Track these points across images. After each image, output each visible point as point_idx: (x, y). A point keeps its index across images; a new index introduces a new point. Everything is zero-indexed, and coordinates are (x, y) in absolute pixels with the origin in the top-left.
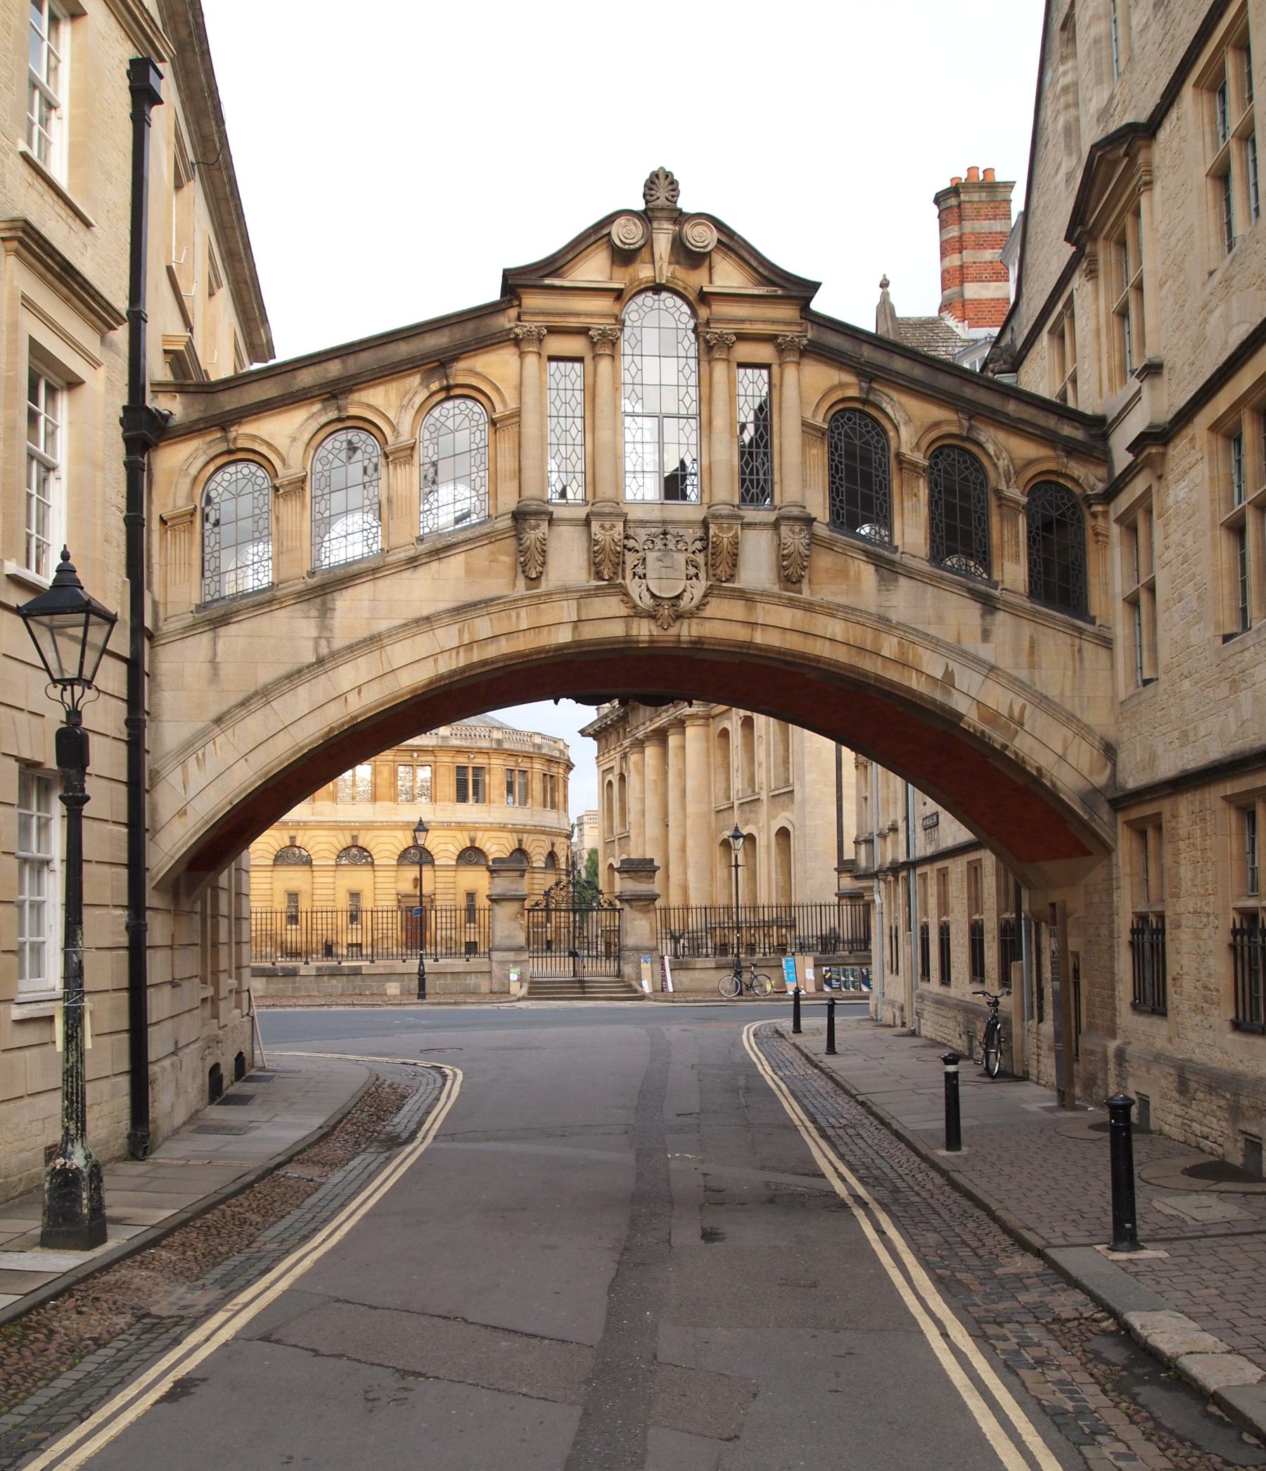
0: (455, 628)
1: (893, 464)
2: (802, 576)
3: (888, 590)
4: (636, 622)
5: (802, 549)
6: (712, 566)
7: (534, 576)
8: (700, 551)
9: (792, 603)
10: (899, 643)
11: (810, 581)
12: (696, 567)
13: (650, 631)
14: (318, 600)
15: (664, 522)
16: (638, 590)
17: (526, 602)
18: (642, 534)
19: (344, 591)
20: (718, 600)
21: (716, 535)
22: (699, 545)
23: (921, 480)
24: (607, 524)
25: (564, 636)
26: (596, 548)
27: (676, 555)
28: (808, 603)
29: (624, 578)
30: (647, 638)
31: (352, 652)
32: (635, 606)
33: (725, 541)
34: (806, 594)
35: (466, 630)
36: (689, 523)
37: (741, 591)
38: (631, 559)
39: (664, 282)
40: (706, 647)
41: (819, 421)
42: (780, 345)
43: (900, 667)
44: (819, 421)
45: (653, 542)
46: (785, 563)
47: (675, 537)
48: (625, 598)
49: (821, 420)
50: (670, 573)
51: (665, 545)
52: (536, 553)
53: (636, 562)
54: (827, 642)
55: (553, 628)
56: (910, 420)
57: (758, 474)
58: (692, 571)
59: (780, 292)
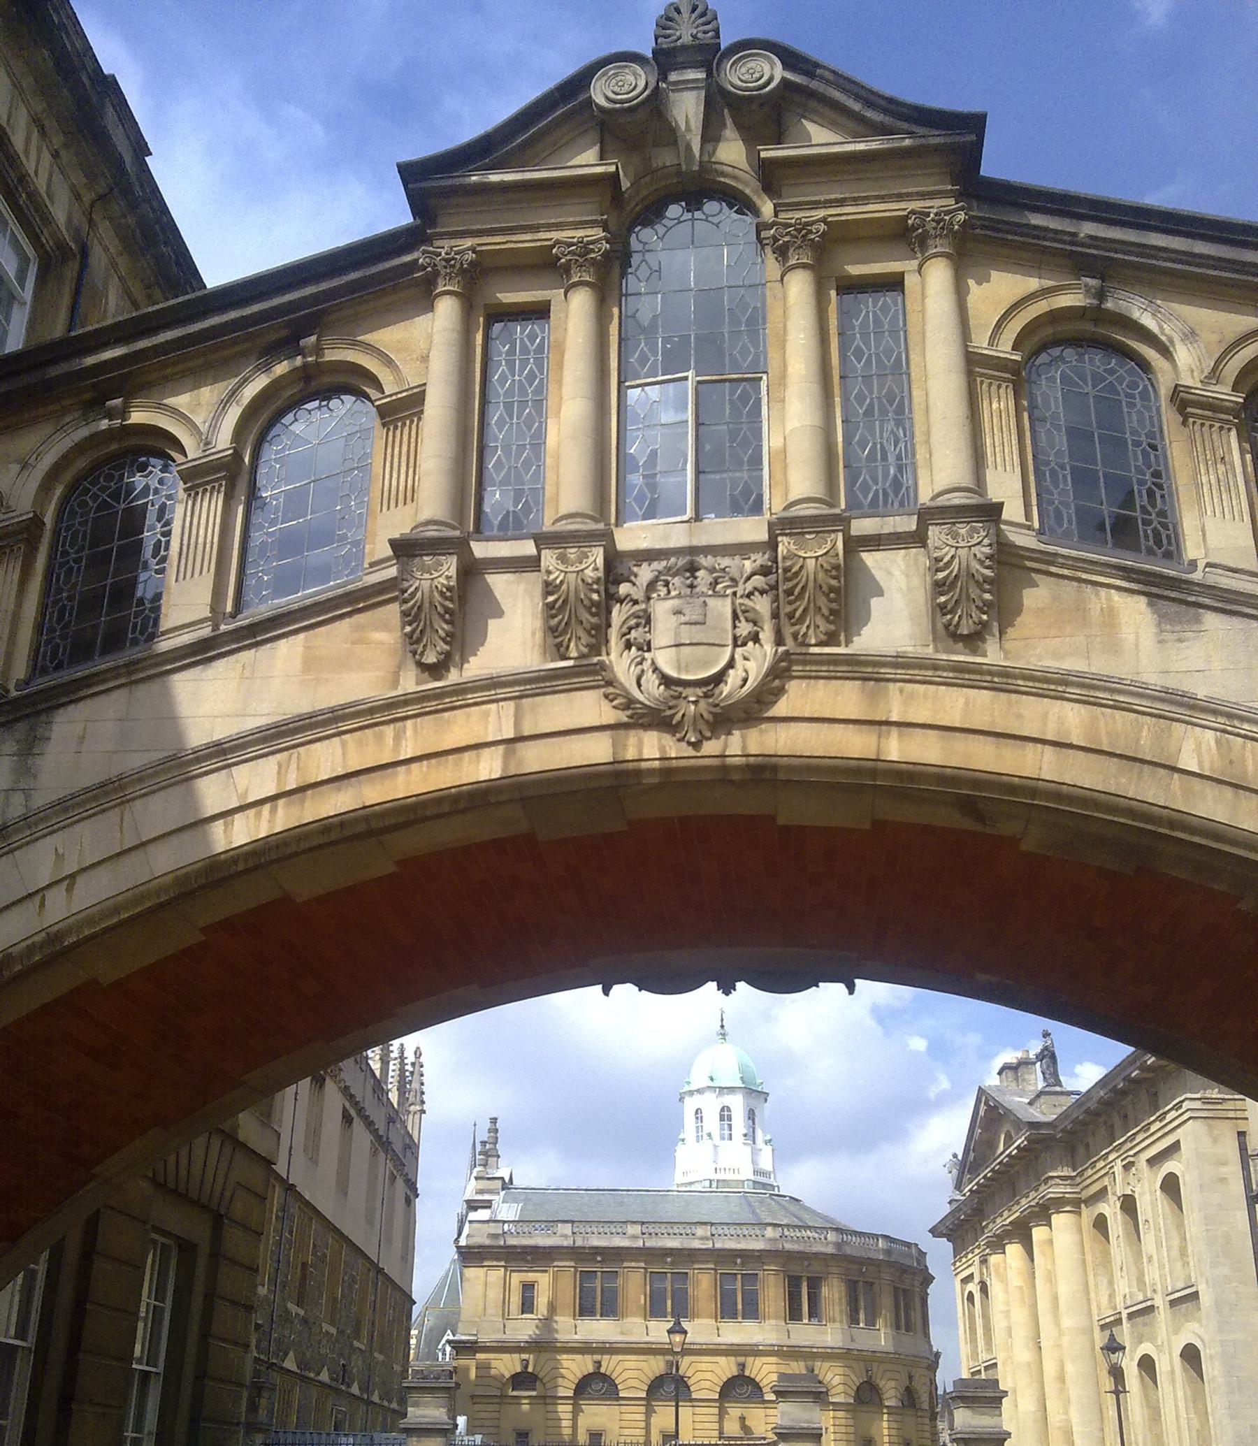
0: (272, 761)
1: (1169, 417)
2: (985, 625)
3: (1180, 640)
4: (632, 737)
5: (975, 566)
6: (791, 616)
7: (431, 658)
8: (762, 592)
9: (966, 676)
10: (1218, 742)
11: (1001, 633)
12: (755, 623)
13: (662, 748)
14: (21, 727)
15: (693, 550)
16: (635, 671)
17: (412, 710)
18: (645, 573)
19: (71, 707)
20: (804, 683)
21: (790, 556)
22: (758, 581)
23: (1233, 433)
24: (572, 553)
25: (488, 768)
26: (551, 599)
27: (712, 602)
28: (1000, 674)
29: (608, 654)
30: (656, 764)
31: (66, 810)
32: (630, 703)
33: (811, 564)
34: (992, 655)
35: (293, 766)
36: (742, 549)
37: (852, 660)
38: (618, 614)
39: (696, 168)
40: (781, 776)
41: (1005, 349)
42: (914, 228)
43: (1228, 792)
44: (1005, 349)
45: (667, 584)
46: (943, 599)
47: (712, 570)
48: (611, 690)
49: (1009, 349)
50: (698, 634)
51: (692, 586)
52: (436, 618)
53: (633, 622)
54: (1049, 750)
55: (467, 755)
56: (1193, 333)
57: (884, 458)
58: (744, 629)
59: (907, 142)
